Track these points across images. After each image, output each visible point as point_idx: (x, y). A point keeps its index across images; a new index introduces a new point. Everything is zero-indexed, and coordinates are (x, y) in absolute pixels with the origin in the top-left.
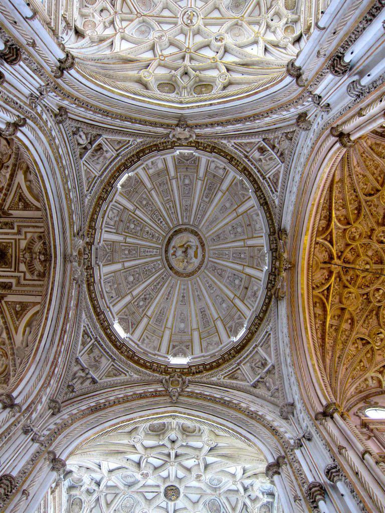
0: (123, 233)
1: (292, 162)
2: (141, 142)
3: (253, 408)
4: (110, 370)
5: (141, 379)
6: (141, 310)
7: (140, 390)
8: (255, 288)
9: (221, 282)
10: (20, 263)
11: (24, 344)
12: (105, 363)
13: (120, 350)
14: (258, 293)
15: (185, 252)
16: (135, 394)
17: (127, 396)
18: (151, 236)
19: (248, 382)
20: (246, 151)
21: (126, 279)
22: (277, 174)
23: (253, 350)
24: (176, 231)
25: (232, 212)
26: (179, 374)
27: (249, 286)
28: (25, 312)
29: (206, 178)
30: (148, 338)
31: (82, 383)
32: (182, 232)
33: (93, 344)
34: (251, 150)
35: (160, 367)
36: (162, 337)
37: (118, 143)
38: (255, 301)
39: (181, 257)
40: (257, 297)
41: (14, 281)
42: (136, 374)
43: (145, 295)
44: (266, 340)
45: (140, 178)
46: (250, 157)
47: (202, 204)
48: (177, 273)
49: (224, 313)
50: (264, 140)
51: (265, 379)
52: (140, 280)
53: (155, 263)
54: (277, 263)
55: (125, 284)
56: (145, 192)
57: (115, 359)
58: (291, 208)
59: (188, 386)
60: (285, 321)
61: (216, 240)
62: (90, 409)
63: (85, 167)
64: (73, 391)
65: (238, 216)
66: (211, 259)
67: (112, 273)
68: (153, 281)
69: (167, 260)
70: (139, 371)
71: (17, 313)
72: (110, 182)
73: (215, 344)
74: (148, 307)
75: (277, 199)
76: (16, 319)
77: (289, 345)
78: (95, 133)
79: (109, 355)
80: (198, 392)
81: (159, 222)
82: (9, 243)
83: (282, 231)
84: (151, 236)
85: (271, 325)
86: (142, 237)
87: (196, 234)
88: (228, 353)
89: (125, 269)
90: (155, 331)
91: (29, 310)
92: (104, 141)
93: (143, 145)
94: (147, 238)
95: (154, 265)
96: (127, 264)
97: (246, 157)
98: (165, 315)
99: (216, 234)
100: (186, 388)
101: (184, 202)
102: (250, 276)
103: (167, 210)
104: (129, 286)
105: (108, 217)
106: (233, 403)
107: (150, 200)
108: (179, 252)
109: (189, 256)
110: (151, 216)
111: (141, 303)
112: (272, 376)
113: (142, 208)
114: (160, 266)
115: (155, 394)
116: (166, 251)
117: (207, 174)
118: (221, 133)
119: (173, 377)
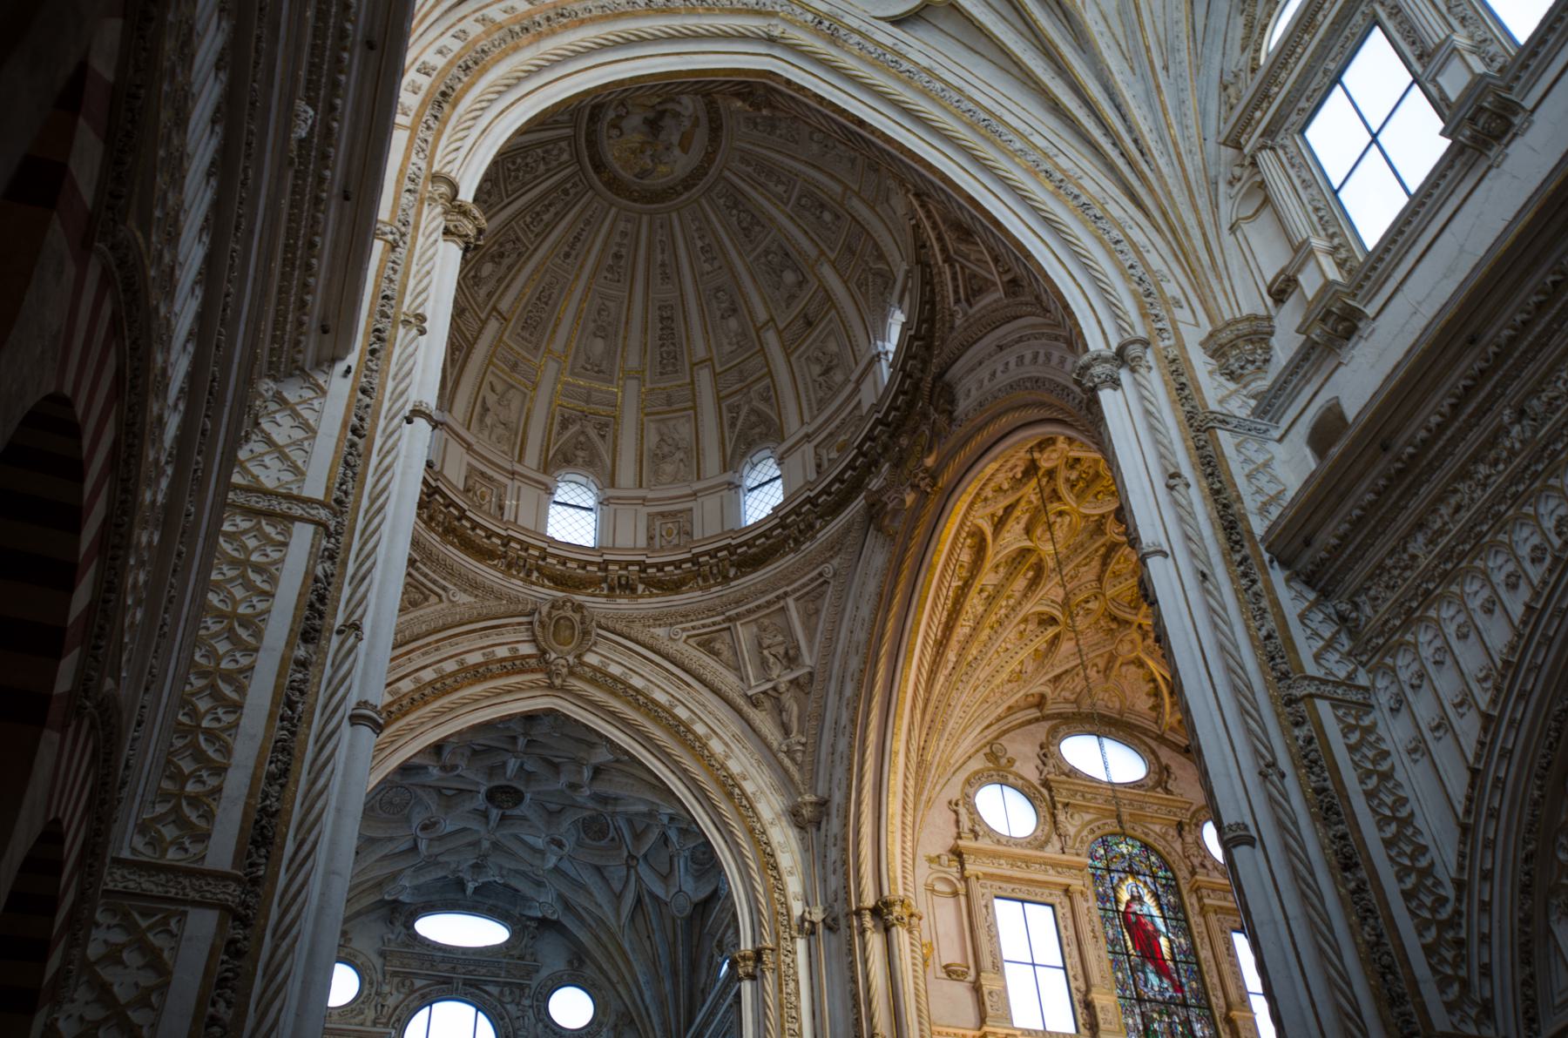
3: (734, 767)
6: (483, 292)
9: (740, 254)
14: (838, 377)
42: (465, 591)
44: (813, 590)
48: (614, 184)
60: (872, 586)
69: (592, 143)
83: (945, 394)
85: (836, 562)
102: (828, 297)
106: (694, 733)
109: (662, 136)
112: (801, 695)
114: (565, 157)
115: (514, 665)
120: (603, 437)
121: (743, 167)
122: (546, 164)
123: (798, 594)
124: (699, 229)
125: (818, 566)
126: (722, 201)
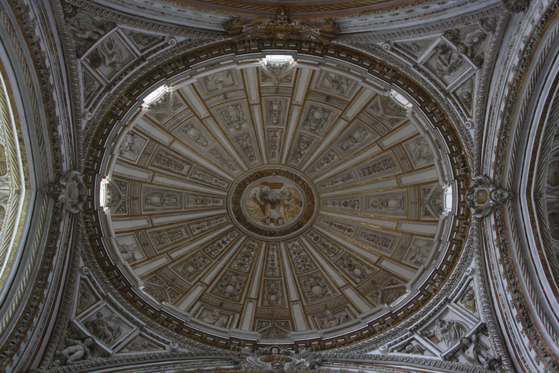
0: (242, 302)
1: (114, 9)
2: (85, 260)
4: (463, 305)
5: (478, 253)
6: (368, 272)
7: (495, 253)
8: (327, 83)
9: (320, 143)
13: (431, 294)
14: (333, 76)
15: (274, 204)
16: (502, 261)
17: (506, 272)
18: (247, 259)
19: (475, 74)
20: (99, 89)
21: (317, 297)
22: (134, 37)
23: (423, 71)
24: (238, 219)
25: (205, 125)
26: (467, 192)
27: (325, 95)
29: (149, 167)
30: (413, 258)
31: (487, 349)
32: (240, 209)
33: (422, 335)
34: (98, 80)
35: (458, 227)
36: (412, 234)
37: (85, 297)
38: (347, 79)
39: (282, 209)
40: (340, 77)
42: (469, 264)
43: (345, 267)
44: (405, 51)
45: (150, 274)
46: (109, 82)
47: (193, 176)
48: (307, 216)
49: (369, 135)
50: (79, 56)
51: (468, 45)
52: (319, 276)
53: (292, 252)
54: (280, 36)
55: (325, 299)
56: (173, 267)
57: (447, 299)
58: (189, 12)
59: (486, 175)
60: (372, 18)
61: (253, 154)
62: (529, 330)
63: (123, 351)
64: (499, 361)
65: (211, 115)
66: (283, 162)
67: (307, 319)
68: (321, 255)
69: (287, 232)
70: (466, 258)
72: (153, 315)
73: (419, 144)
74: (363, 260)
75: (176, 37)
77: (410, 8)
78: (65, 332)
79: (439, 308)
80: (494, 156)
81: (224, 246)
84: (247, 259)
85: (380, 44)
86: (248, 273)
87: (242, 186)
88: (430, 115)
89: (301, 300)
90: (402, 247)
92: (81, 318)
93: (90, 257)
94: (251, 265)
95: (295, 253)
96: (294, 296)
97: (109, 88)
98: (377, 232)
99: (242, 153)
100: (489, 178)
101: (191, 205)
102: (308, 92)
103: (204, 234)
104: (330, 292)
105: (213, 324)
107: (187, 260)
108: (274, 213)
110: (214, 259)
111: (357, 272)
112: (461, 34)
113: (200, 272)
114: (297, 243)
115: (500, 227)
117: (142, 164)
118: (70, 128)
119: (473, 203)
120: (429, 190)
121: (277, 155)
122: (301, 252)
123: (413, 59)
124: (319, 167)
125: (389, 54)
126: (299, 160)
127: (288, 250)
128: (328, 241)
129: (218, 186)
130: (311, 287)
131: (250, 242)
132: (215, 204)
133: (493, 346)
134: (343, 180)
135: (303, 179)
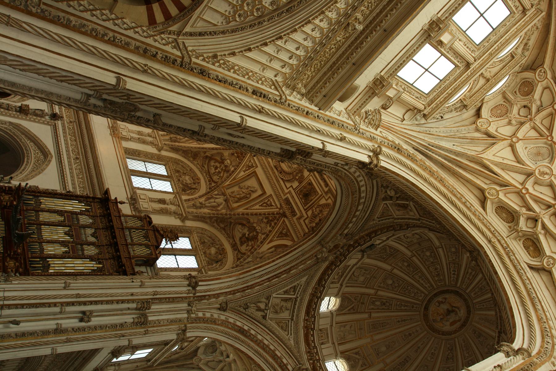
6: (372, 307)
10: (311, 210)
11: (261, 255)
12: (286, 315)
15: (449, 312)
18: (436, 273)
24: (458, 292)
28: (285, 238)
33: (291, 298)
41: (299, 214)
43: (387, 302)
48: (426, 316)
53: (419, 292)
57: (293, 320)
68: (403, 300)
69: (429, 301)
71: (281, 233)
76: (277, 236)
82: (317, 192)
87: (469, 312)
91: (287, 240)
94: (431, 272)
95: (417, 292)
108: (445, 307)
110: (449, 263)
111: (378, 303)
114: (421, 298)
116: (436, 295)
122: (415, 295)
126: (449, 346)
127: (422, 292)
128: (406, 309)
129: (480, 304)
130: (394, 282)
131: (443, 283)
132: (474, 292)
133: (254, 313)
134: (419, 348)
135: (441, 336)
